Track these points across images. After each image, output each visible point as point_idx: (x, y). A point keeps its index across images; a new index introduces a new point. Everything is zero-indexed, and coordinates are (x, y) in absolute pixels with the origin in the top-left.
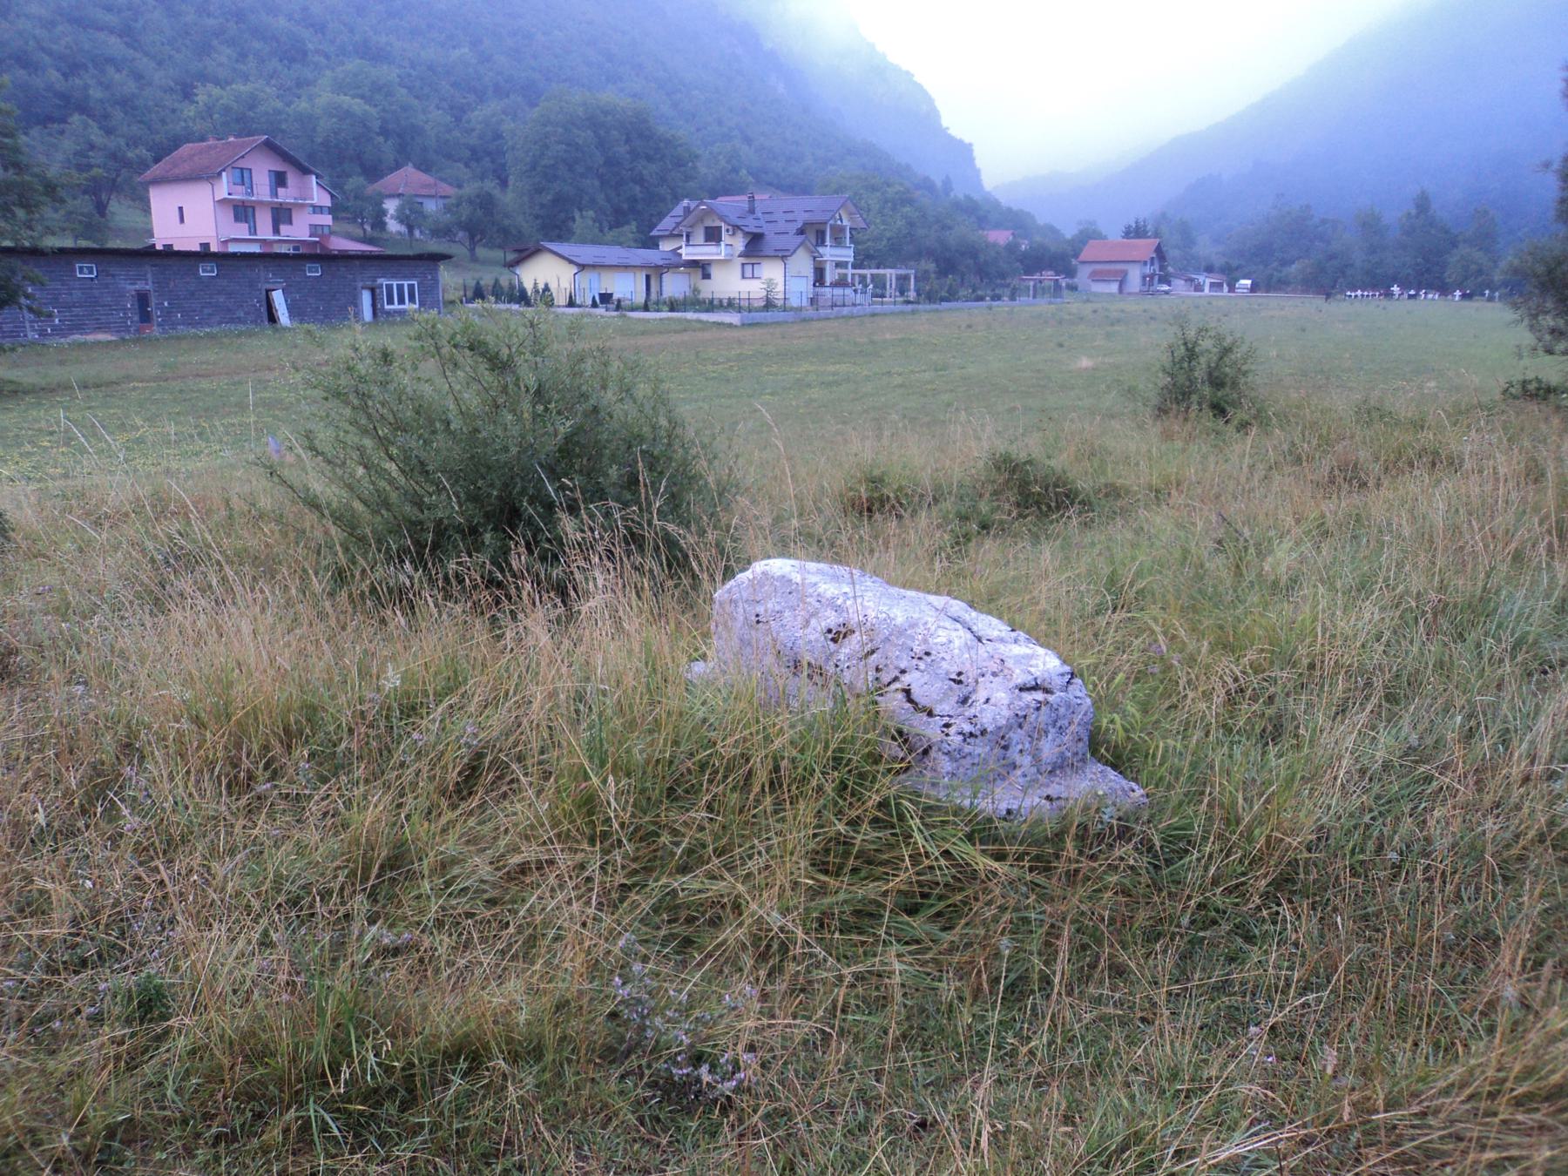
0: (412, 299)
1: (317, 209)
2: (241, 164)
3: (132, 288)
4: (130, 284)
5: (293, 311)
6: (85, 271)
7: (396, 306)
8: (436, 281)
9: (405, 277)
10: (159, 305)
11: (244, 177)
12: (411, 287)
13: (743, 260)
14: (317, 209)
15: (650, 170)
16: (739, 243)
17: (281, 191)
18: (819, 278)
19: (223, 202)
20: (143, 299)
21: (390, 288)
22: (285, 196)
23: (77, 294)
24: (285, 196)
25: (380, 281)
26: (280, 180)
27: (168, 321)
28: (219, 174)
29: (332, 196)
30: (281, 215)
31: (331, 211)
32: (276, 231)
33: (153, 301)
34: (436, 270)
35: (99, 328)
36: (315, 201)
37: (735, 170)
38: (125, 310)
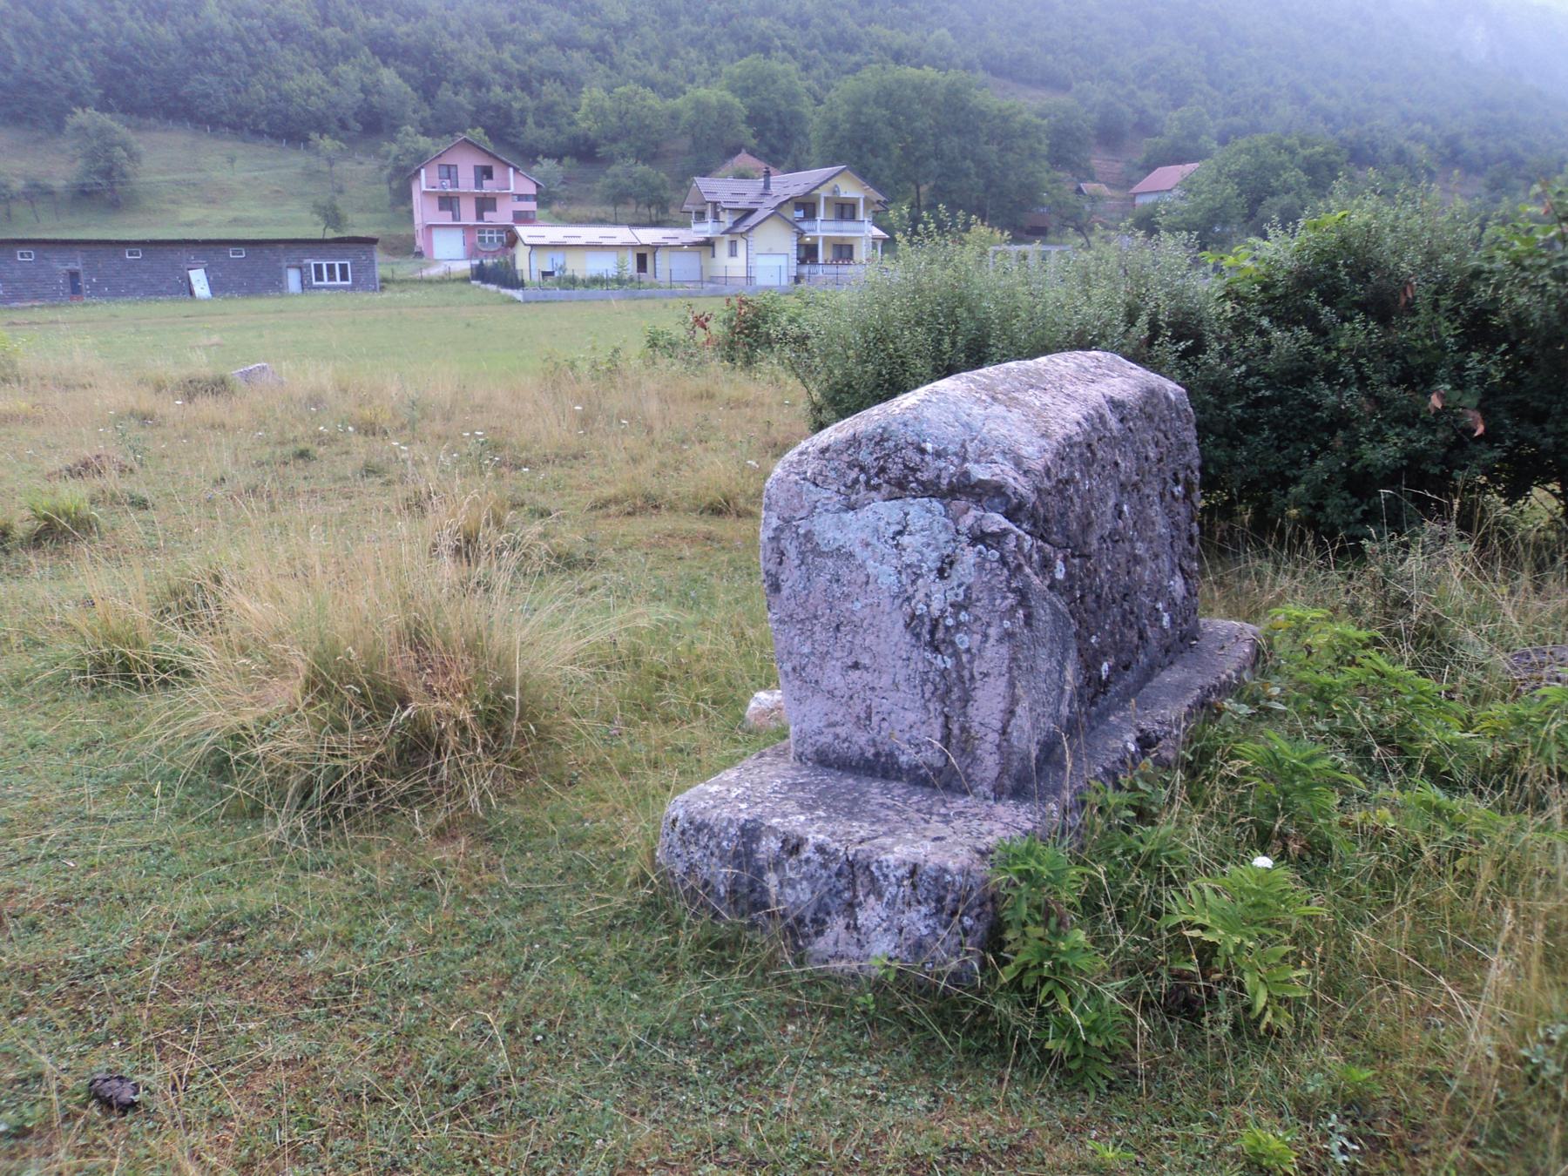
0: (344, 277)
1: (522, 197)
2: (446, 161)
4: (61, 265)
5: (216, 287)
6: (25, 257)
7: (326, 282)
8: (372, 262)
9: (323, 257)
10: (89, 282)
11: (450, 172)
12: (343, 268)
13: (727, 237)
14: (522, 197)
15: (951, 144)
16: (727, 220)
17: (486, 182)
18: (808, 254)
19: (425, 193)
20: (74, 276)
21: (318, 268)
22: (489, 187)
23: (18, 273)
24: (489, 187)
25: (306, 261)
26: (486, 173)
27: (96, 291)
28: (418, 172)
29: (538, 186)
30: (485, 204)
31: (535, 198)
32: (480, 217)
33: (83, 277)
34: (371, 252)
36: (512, 190)
37: (1194, 137)
38: (57, 284)
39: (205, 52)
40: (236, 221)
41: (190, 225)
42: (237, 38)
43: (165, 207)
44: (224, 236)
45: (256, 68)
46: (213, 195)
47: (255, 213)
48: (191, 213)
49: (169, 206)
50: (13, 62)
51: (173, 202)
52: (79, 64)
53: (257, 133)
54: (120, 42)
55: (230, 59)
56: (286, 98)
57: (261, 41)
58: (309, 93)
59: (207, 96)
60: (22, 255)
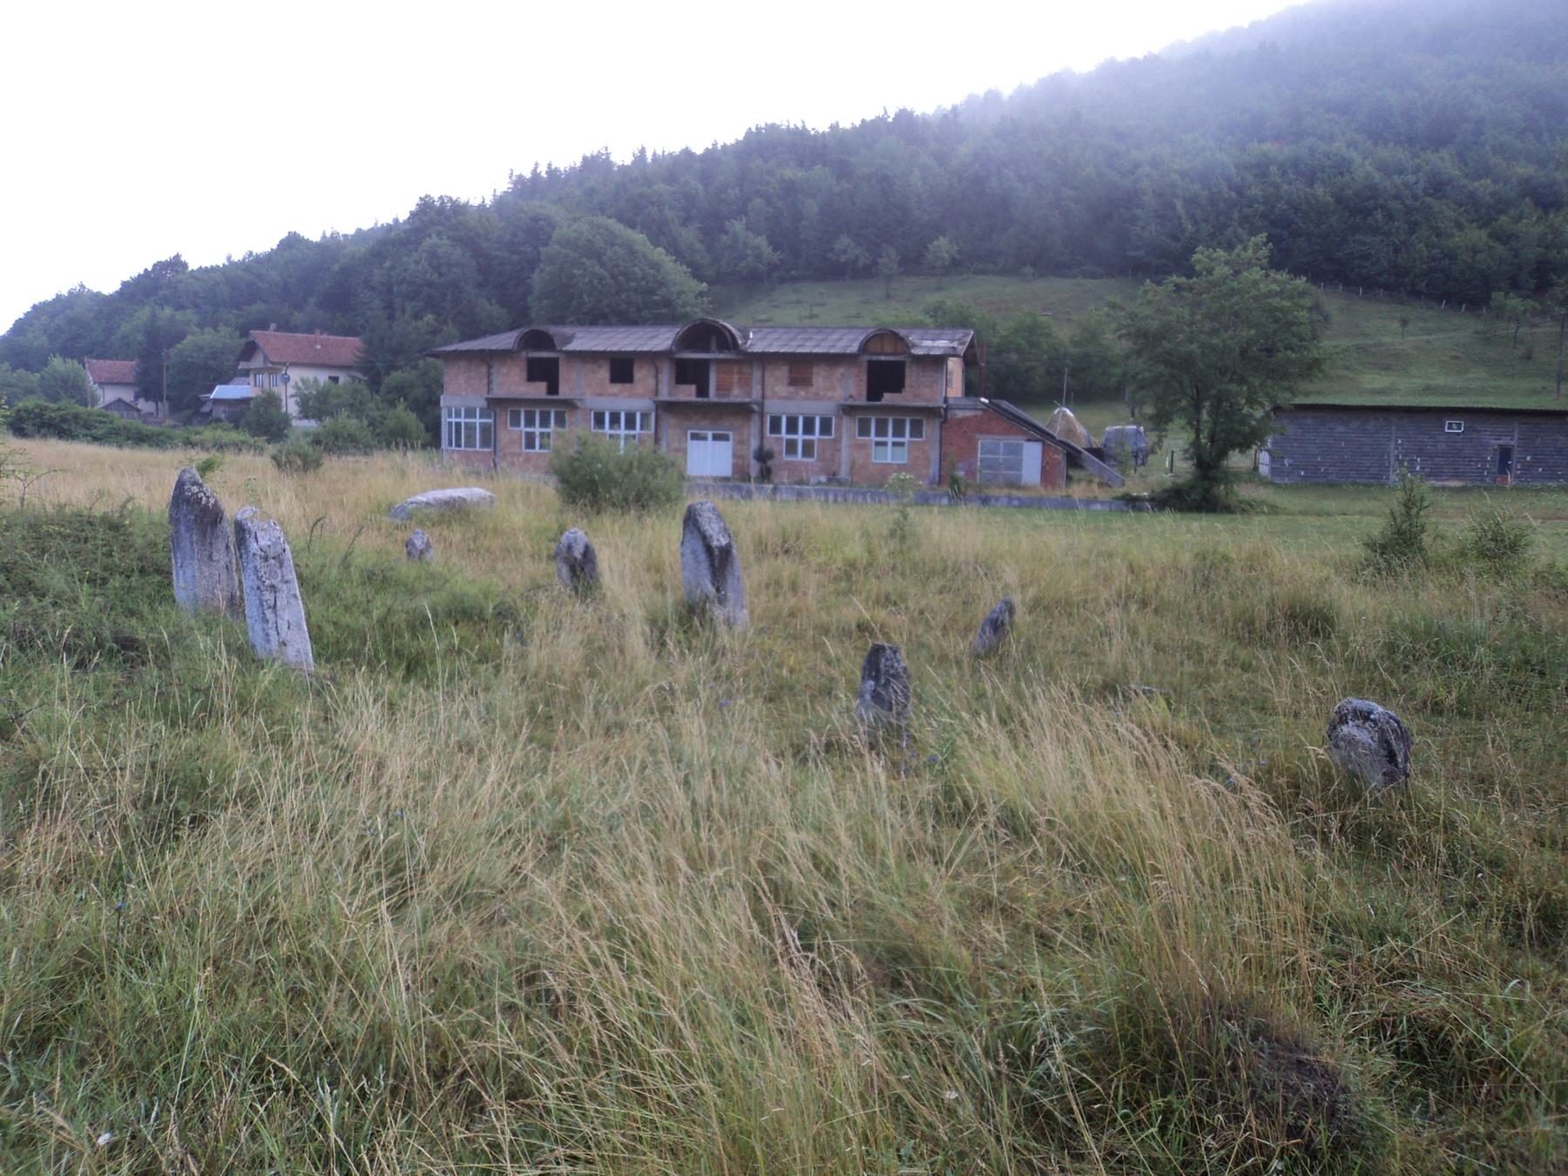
3: (1495, 443)
4: (1493, 438)
6: (1453, 427)
20: (1505, 453)
23: (1442, 446)
33: (1516, 455)
35: (1456, 476)
39: (1367, 213)
40: (1428, 390)
41: (1381, 392)
42: (1397, 197)
43: (1340, 373)
44: (1533, 407)
45: (1413, 227)
46: (1389, 362)
47: (1441, 380)
48: (1380, 381)
49: (1346, 373)
50: (1183, 231)
51: (1347, 368)
52: (1240, 230)
53: (1416, 294)
54: (1282, 205)
55: (1390, 217)
56: (1451, 255)
57: (1415, 198)
58: (1475, 251)
59: (1366, 257)
60: (1450, 427)
